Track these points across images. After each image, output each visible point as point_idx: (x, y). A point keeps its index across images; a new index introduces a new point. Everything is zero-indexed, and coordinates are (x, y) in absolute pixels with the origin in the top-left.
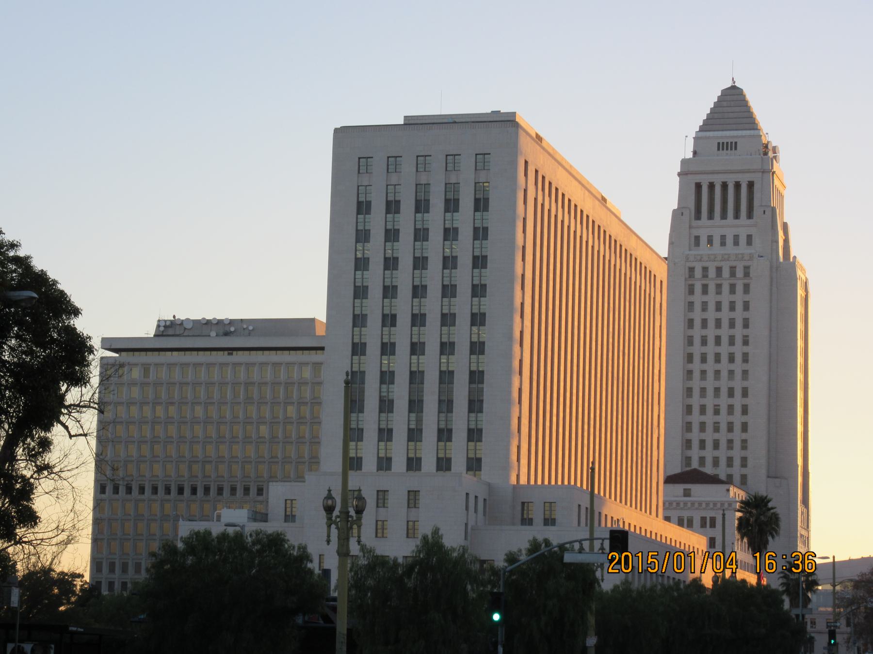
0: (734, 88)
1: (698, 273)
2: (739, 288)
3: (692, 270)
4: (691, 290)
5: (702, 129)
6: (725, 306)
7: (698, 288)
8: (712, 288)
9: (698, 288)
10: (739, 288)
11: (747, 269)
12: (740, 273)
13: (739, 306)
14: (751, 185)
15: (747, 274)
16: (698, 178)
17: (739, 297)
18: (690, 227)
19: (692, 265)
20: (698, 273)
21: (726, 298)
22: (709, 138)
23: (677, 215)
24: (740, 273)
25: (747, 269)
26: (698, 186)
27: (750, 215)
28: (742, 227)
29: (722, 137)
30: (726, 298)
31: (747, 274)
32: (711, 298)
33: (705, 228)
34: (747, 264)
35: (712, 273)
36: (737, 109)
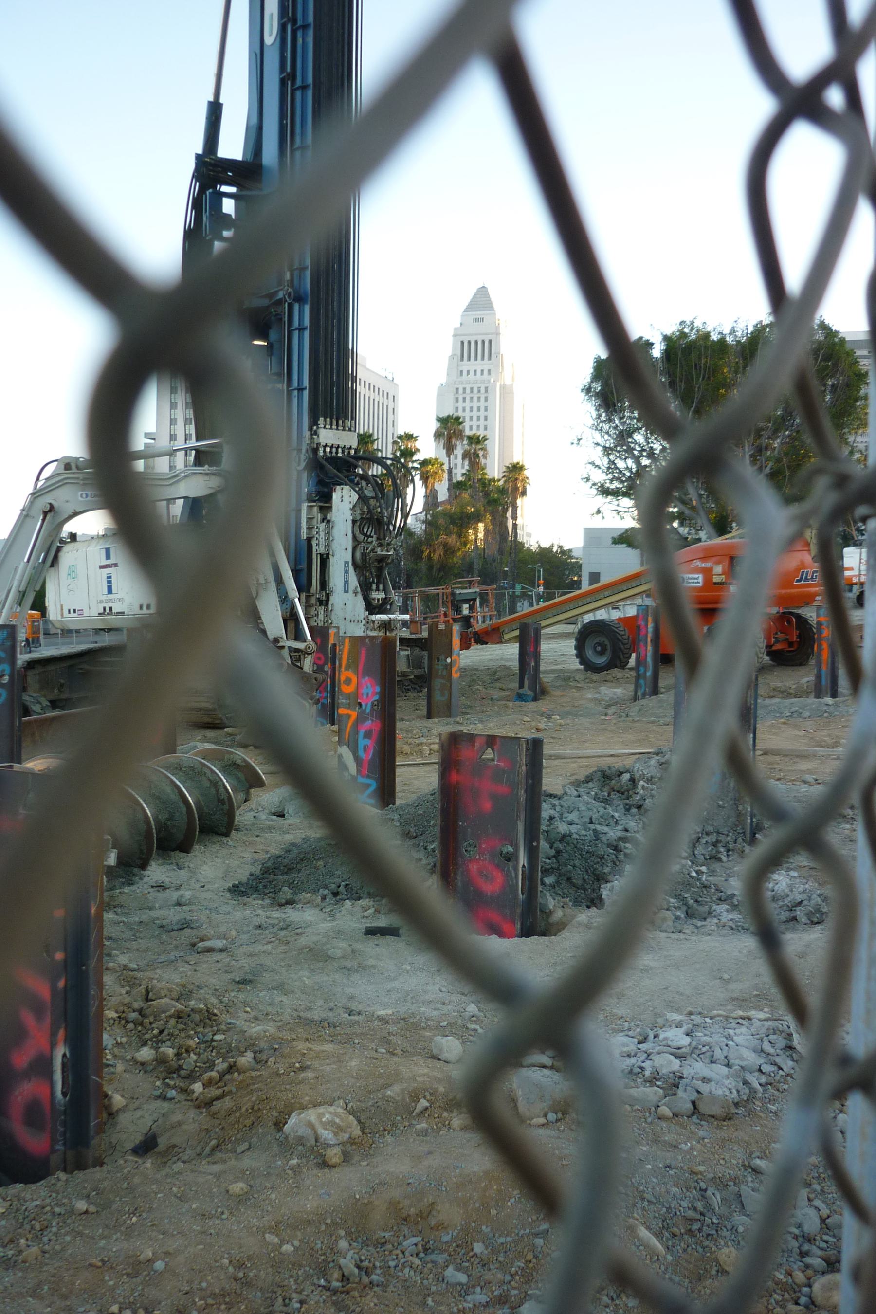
0: (483, 287)
1: (461, 391)
2: (482, 399)
3: (457, 389)
4: (457, 400)
5: (465, 311)
6: (475, 409)
7: (461, 400)
8: (468, 399)
9: (461, 400)
10: (482, 399)
11: (486, 388)
12: (483, 390)
13: (482, 409)
14: (490, 341)
15: (486, 391)
16: (462, 338)
17: (482, 404)
18: (458, 365)
19: (458, 386)
20: (461, 391)
21: (475, 404)
22: (468, 315)
23: (452, 357)
24: (483, 390)
25: (486, 388)
26: (462, 343)
27: (490, 358)
28: (485, 365)
29: (476, 315)
30: (475, 404)
31: (486, 391)
32: (468, 405)
33: (466, 366)
34: (487, 385)
35: (468, 391)
36: (485, 299)
